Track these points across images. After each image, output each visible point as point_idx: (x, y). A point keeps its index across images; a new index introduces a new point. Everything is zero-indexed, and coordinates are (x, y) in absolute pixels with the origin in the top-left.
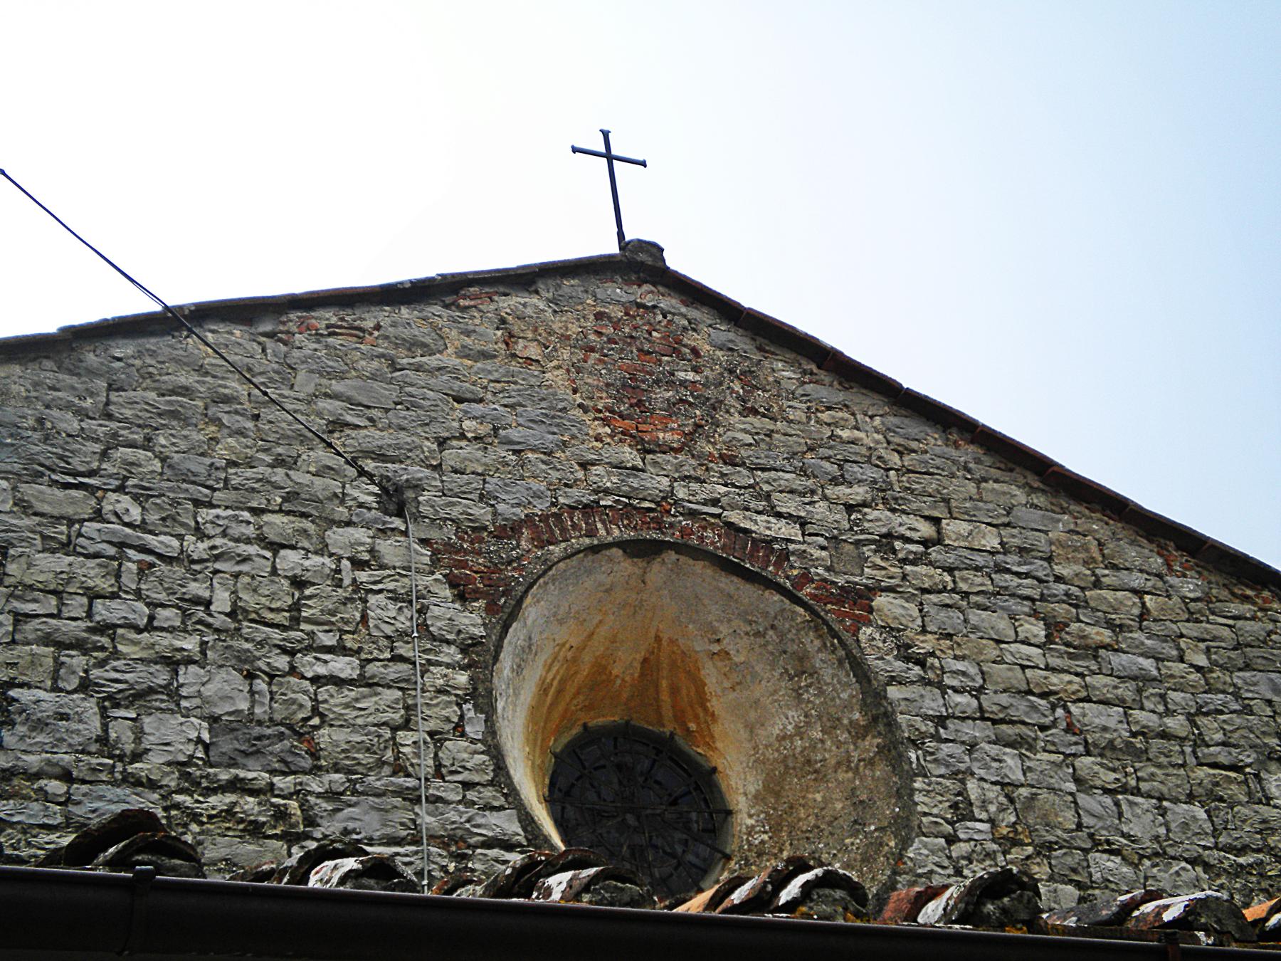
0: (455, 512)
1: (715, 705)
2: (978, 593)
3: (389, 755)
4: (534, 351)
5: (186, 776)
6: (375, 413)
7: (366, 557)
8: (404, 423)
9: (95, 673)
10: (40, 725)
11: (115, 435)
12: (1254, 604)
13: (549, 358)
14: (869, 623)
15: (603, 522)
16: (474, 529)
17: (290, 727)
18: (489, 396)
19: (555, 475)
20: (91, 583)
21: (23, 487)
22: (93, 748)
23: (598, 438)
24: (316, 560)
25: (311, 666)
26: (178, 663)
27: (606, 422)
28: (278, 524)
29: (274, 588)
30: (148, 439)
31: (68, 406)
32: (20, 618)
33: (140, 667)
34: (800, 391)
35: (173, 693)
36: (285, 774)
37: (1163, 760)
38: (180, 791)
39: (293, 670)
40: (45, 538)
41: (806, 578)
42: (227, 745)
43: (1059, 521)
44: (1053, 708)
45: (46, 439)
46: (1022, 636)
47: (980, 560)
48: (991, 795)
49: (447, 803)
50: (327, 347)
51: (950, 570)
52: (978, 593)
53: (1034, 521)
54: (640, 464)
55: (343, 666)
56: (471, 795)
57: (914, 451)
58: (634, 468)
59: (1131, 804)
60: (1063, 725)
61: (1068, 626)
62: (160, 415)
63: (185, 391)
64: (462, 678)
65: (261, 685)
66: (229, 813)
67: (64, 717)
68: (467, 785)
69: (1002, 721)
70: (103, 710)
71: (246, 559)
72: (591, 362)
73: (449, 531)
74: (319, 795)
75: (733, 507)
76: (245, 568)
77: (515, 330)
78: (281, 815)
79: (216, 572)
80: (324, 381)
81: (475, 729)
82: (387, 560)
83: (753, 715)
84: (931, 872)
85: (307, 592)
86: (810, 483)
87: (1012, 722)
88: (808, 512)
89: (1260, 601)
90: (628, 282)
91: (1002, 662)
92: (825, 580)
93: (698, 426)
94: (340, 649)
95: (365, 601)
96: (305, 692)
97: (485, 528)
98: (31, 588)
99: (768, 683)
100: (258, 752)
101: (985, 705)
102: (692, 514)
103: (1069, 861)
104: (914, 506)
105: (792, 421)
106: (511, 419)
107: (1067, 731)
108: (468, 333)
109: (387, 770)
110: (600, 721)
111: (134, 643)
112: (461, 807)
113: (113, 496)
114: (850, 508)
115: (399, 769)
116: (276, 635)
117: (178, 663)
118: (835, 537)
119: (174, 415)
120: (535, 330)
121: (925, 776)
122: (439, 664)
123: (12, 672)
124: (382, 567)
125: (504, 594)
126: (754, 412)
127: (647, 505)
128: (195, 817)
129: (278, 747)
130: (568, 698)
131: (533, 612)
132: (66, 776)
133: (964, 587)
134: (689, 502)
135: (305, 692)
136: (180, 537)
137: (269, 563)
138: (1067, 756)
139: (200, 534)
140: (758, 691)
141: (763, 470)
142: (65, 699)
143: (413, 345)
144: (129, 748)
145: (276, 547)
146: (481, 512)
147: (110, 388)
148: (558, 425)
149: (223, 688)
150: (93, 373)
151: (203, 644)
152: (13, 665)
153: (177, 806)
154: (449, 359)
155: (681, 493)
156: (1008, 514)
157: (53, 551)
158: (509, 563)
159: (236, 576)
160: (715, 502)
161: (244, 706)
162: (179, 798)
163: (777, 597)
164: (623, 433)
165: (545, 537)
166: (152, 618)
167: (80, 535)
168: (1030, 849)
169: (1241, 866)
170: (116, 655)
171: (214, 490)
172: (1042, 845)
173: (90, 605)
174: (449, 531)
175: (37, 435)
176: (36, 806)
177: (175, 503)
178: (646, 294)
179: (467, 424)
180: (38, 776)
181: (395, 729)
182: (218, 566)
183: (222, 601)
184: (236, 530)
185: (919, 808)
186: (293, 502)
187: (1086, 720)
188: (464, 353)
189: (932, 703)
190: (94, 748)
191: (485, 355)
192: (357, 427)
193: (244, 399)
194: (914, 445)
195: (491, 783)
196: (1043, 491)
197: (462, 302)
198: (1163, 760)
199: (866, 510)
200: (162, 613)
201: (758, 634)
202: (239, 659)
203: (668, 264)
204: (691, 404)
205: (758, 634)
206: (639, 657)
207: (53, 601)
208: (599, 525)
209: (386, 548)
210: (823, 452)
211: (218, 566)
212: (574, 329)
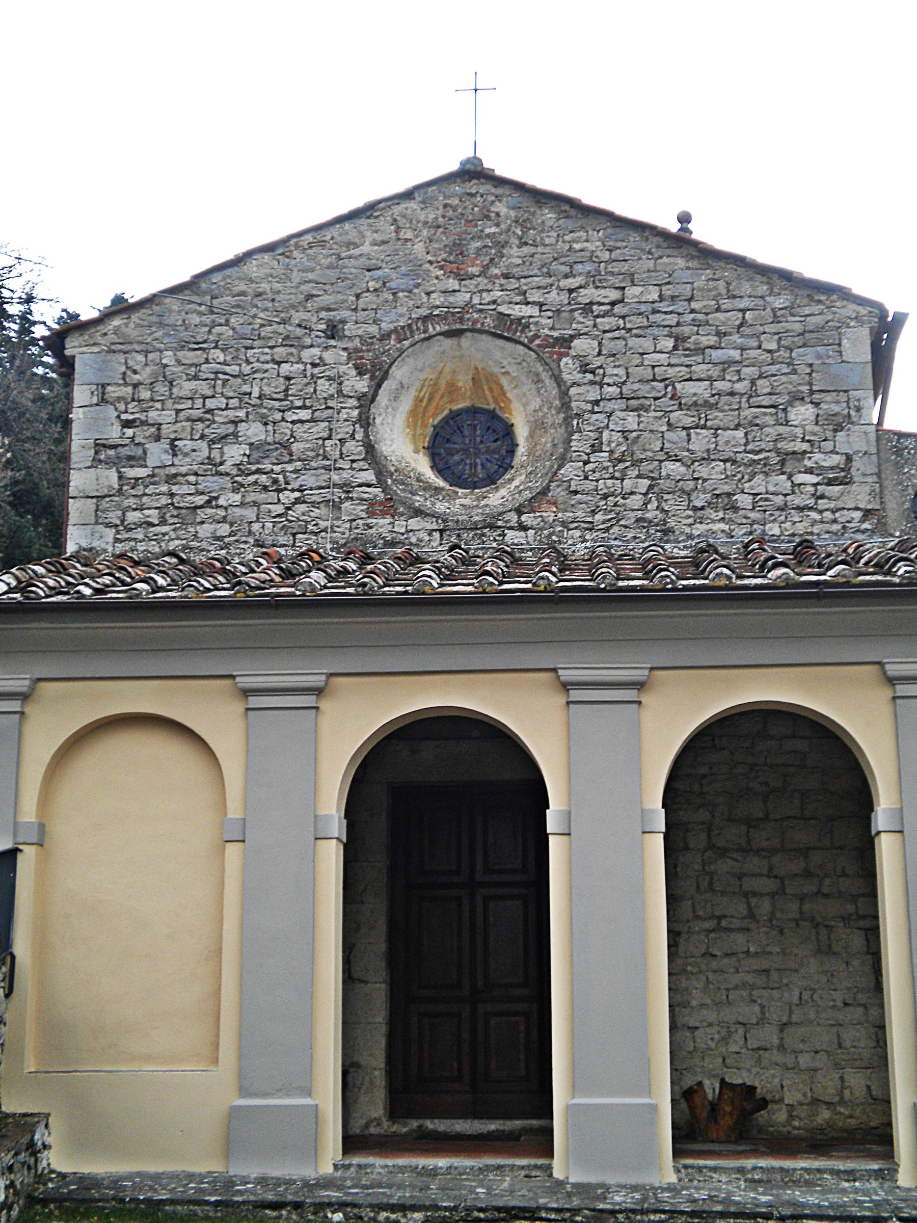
0: (360, 332)
1: (509, 395)
2: (636, 328)
3: (321, 452)
4: (409, 235)
5: (239, 469)
6: (327, 287)
7: (318, 361)
8: (339, 290)
9: (207, 431)
10: (186, 455)
11: (214, 321)
12: (824, 304)
13: (417, 236)
14: (567, 355)
15: (432, 324)
16: (370, 338)
17: (280, 444)
18: (384, 265)
19: (412, 302)
20: (203, 393)
21: (178, 353)
22: (206, 461)
23: (437, 278)
24: (296, 366)
25: (290, 417)
26: (237, 422)
27: (441, 268)
28: (280, 352)
29: (277, 383)
30: (227, 321)
31: (195, 311)
32: (178, 411)
33: (223, 426)
34: (556, 225)
35: (235, 435)
36: (278, 464)
37: (726, 407)
38: (237, 476)
39: (283, 419)
40: (187, 374)
41: (536, 336)
42: (255, 455)
43: (702, 274)
44: (666, 387)
45: (186, 330)
46: (658, 349)
47: (643, 308)
48: (614, 438)
49: (344, 469)
50: (307, 255)
51: (623, 317)
52: (636, 328)
53: (687, 278)
54: (457, 288)
55: (305, 415)
56: (354, 465)
57: (619, 248)
58: (454, 291)
59: (698, 434)
60: (669, 395)
61: (689, 338)
62: (233, 307)
63: (243, 293)
64: (356, 413)
65: (270, 428)
66: (256, 483)
67: (194, 451)
68: (353, 461)
69: (632, 398)
70: (209, 445)
71: (266, 371)
72: (438, 234)
73: (357, 343)
74: (291, 472)
75: (503, 303)
76: (266, 375)
77: (401, 224)
78: (275, 481)
79: (254, 379)
80: (304, 275)
81: (359, 436)
82: (327, 362)
83: (524, 400)
84: (571, 479)
85: (292, 382)
86: (549, 280)
87: (638, 398)
88: (546, 298)
89: (828, 303)
90: (464, 182)
91: (642, 365)
92: (547, 335)
93: (492, 260)
94: (304, 407)
95: (316, 383)
96: (288, 428)
97: (375, 337)
98: (181, 398)
99: (528, 386)
100: (267, 456)
101: (624, 391)
102: (481, 311)
103: (651, 467)
104: (610, 283)
105: (547, 245)
106: (394, 275)
107: (671, 399)
108: (376, 232)
109: (321, 458)
110: (460, 406)
111: (221, 416)
112: (349, 471)
113: (212, 351)
114: (571, 291)
115: (326, 458)
116: (277, 404)
117: (237, 422)
118: (558, 310)
119: (238, 306)
120: (411, 222)
121: (580, 432)
122: (345, 408)
123: (176, 435)
124: (325, 365)
125: (379, 369)
126: (526, 244)
127: (457, 310)
128: (242, 486)
129: (275, 454)
130: (437, 400)
131: (398, 373)
132: (196, 474)
133: (628, 326)
134: (481, 304)
135: (288, 428)
136: (240, 365)
137: (276, 371)
138: (666, 412)
139: (248, 362)
140: (525, 389)
141: (525, 277)
142: (195, 443)
143: (350, 245)
144: (218, 460)
145: (279, 363)
146: (373, 329)
147: (213, 298)
148: (416, 275)
149: (254, 431)
150: (205, 293)
151: (247, 413)
152: (176, 431)
153: (236, 482)
154: (366, 248)
155: (476, 300)
156: (670, 275)
157: (190, 380)
158: (384, 353)
159: (262, 379)
160: (494, 302)
161: (263, 437)
162: (237, 479)
163: (522, 347)
164: (450, 272)
165: (402, 337)
166: (227, 404)
167: (200, 371)
168: (628, 464)
169: (754, 461)
170: (214, 422)
171: (254, 340)
172: (637, 461)
173: (204, 402)
174: (357, 343)
175: (183, 328)
176: (185, 487)
177: (237, 350)
178: (473, 186)
179: (371, 284)
180: (186, 475)
181: (324, 440)
182: (255, 376)
183: (255, 393)
184: (262, 358)
185: (573, 449)
187: (684, 391)
188: (374, 243)
189: (593, 394)
190: (206, 461)
191: (384, 242)
192: (319, 296)
193: (268, 291)
194: (619, 244)
195: (363, 459)
196: (698, 257)
197: (376, 214)
198: (726, 407)
199: (581, 290)
200: (231, 401)
201: (519, 364)
202: (262, 417)
203: (485, 166)
204: (490, 247)
205: (519, 364)
206: (470, 377)
207: (190, 402)
208: (430, 326)
209: (328, 356)
210: (563, 260)
211: (255, 376)
212: (432, 216)
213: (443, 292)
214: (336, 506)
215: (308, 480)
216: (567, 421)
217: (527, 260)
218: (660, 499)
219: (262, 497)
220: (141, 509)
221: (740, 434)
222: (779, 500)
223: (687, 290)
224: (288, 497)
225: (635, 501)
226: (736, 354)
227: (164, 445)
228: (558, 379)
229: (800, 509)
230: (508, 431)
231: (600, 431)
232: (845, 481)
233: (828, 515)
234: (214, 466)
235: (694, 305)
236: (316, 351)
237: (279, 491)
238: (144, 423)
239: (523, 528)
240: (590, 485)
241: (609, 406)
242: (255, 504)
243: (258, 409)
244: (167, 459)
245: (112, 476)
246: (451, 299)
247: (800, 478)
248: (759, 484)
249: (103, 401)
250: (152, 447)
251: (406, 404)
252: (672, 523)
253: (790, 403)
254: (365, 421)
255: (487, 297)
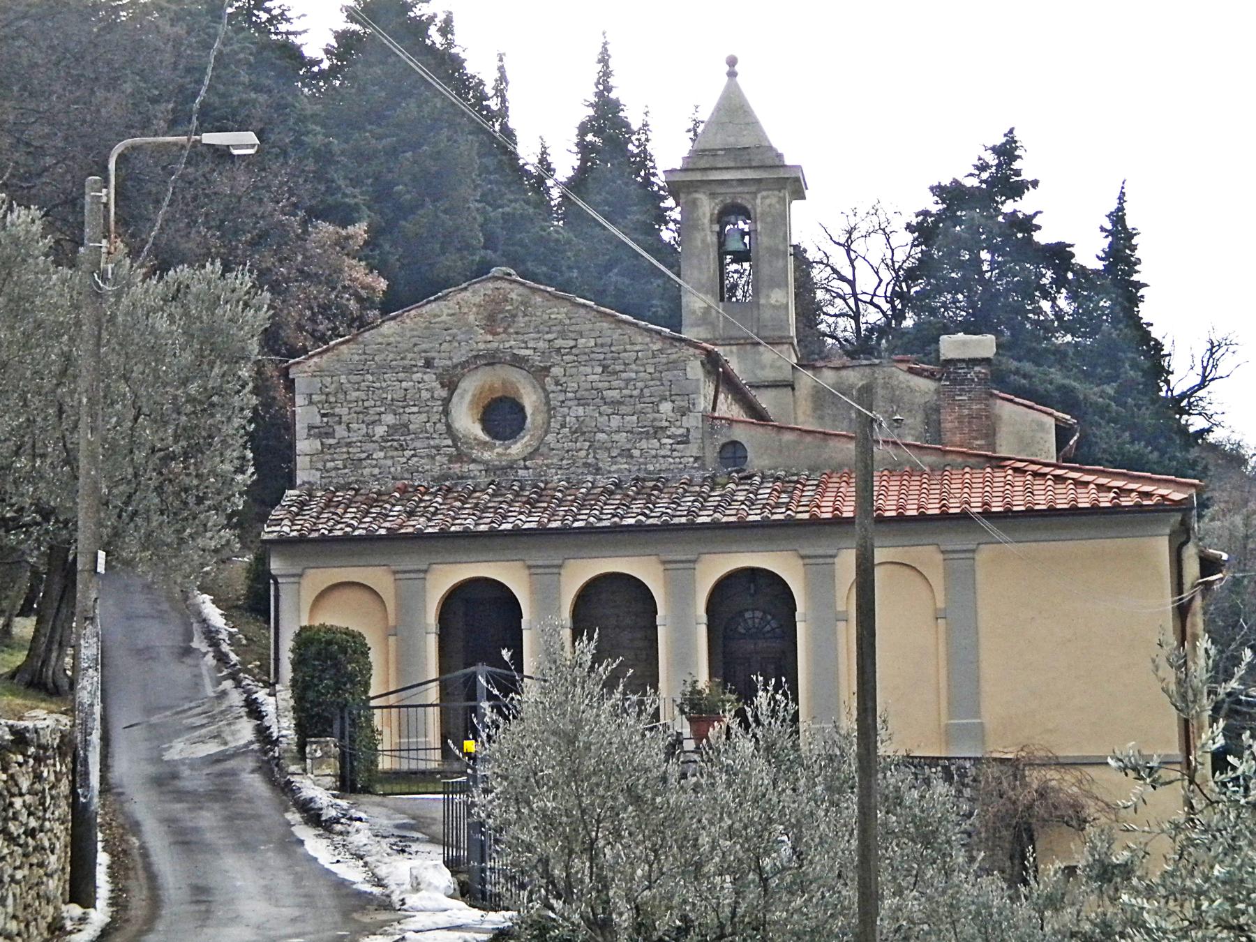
4: (466, 310)
25: (407, 410)
28: (401, 375)
35: (380, 420)
55: (415, 409)
81: (443, 421)
131: (463, 385)
143: (436, 316)
146: (449, 363)
149: (389, 419)
154: (444, 318)
186: (406, 369)
188: (448, 315)
209: (426, 377)
213: (483, 341)
214: (433, 458)
215: (418, 444)
216: (549, 411)
217: (527, 325)
218: (595, 453)
219: (395, 453)
220: (333, 460)
221: (635, 418)
222: (653, 452)
223: (609, 340)
224: (408, 453)
225: (583, 453)
226: (633, 375)
227: (343, 426)
228: (544, 390)
229: (664, 457)
230: (521, 409)
231: (564, 417)
232: (686, 442)
233: (677, 460)
234: (369, 437)
235: (613, 349)
236: (419, 375)
237: (404, 450)
238: (333, 415)
239: (526, 468)
240: (560, 446)
241: (569, 403)
242: (392, 457)
243: (391, 407)
244: (345, 434)
245: (317, 444)
246: (489, 346)
247: (665, 441)
248: (644, 444)
249: (311, 403)
250: (337, 427)
251: (468, 398)
252: (601, 465)
253: (660, 401)
254: (446, 412)
255: (507, 345)
